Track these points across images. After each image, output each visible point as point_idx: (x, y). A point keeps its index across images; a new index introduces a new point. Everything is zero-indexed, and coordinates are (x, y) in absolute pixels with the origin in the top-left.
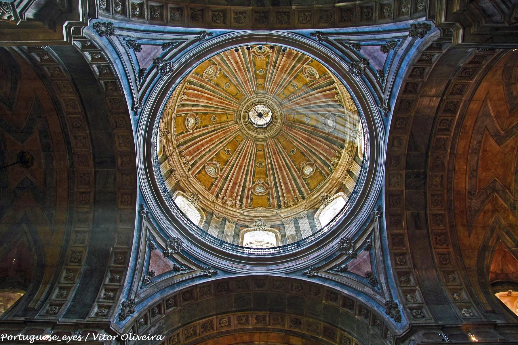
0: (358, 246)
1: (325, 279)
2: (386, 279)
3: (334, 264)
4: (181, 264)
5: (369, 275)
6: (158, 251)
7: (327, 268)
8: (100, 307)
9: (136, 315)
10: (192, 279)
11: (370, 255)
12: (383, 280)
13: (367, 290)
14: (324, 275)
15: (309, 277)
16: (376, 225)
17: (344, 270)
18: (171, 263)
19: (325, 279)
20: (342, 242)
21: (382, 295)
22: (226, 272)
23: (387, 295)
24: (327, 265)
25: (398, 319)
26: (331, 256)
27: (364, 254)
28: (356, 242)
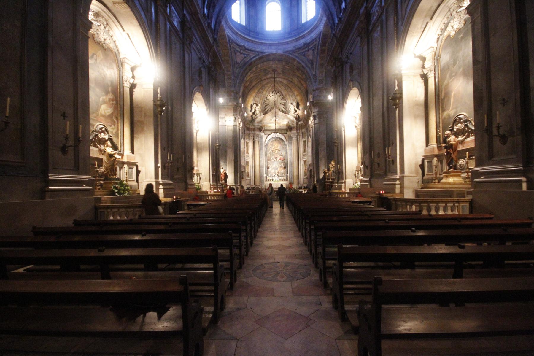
0: (311, 47)
1: (297, 57)
2: (316, 65)
3: (300, 52)
4: (246, 55)
5: (312, 61)
6: (238, 53)
7: (298, 52)
8: (228, 82)
9: (238, 81)
10: (251, 59)
11: (313, 53)
12: (315, 64)
13: (310, 65)
14: (297, 55)
15: (292, 55)
16: (317, 43)
17: (304, 55)
18: (243, 56)
19: (297, 57)
20: (305, 44)
21: (314, 70)
22: (262, 53)
23: (315, 71)
24: (298, 51)
25: (315, 82)
26: (300, 48)
27: (311, 52)
28: (310, 46)
